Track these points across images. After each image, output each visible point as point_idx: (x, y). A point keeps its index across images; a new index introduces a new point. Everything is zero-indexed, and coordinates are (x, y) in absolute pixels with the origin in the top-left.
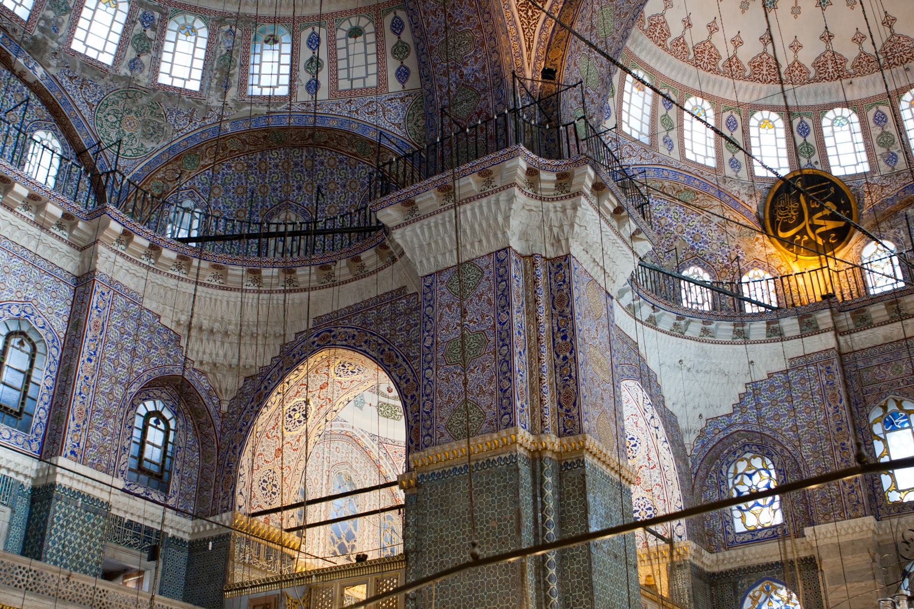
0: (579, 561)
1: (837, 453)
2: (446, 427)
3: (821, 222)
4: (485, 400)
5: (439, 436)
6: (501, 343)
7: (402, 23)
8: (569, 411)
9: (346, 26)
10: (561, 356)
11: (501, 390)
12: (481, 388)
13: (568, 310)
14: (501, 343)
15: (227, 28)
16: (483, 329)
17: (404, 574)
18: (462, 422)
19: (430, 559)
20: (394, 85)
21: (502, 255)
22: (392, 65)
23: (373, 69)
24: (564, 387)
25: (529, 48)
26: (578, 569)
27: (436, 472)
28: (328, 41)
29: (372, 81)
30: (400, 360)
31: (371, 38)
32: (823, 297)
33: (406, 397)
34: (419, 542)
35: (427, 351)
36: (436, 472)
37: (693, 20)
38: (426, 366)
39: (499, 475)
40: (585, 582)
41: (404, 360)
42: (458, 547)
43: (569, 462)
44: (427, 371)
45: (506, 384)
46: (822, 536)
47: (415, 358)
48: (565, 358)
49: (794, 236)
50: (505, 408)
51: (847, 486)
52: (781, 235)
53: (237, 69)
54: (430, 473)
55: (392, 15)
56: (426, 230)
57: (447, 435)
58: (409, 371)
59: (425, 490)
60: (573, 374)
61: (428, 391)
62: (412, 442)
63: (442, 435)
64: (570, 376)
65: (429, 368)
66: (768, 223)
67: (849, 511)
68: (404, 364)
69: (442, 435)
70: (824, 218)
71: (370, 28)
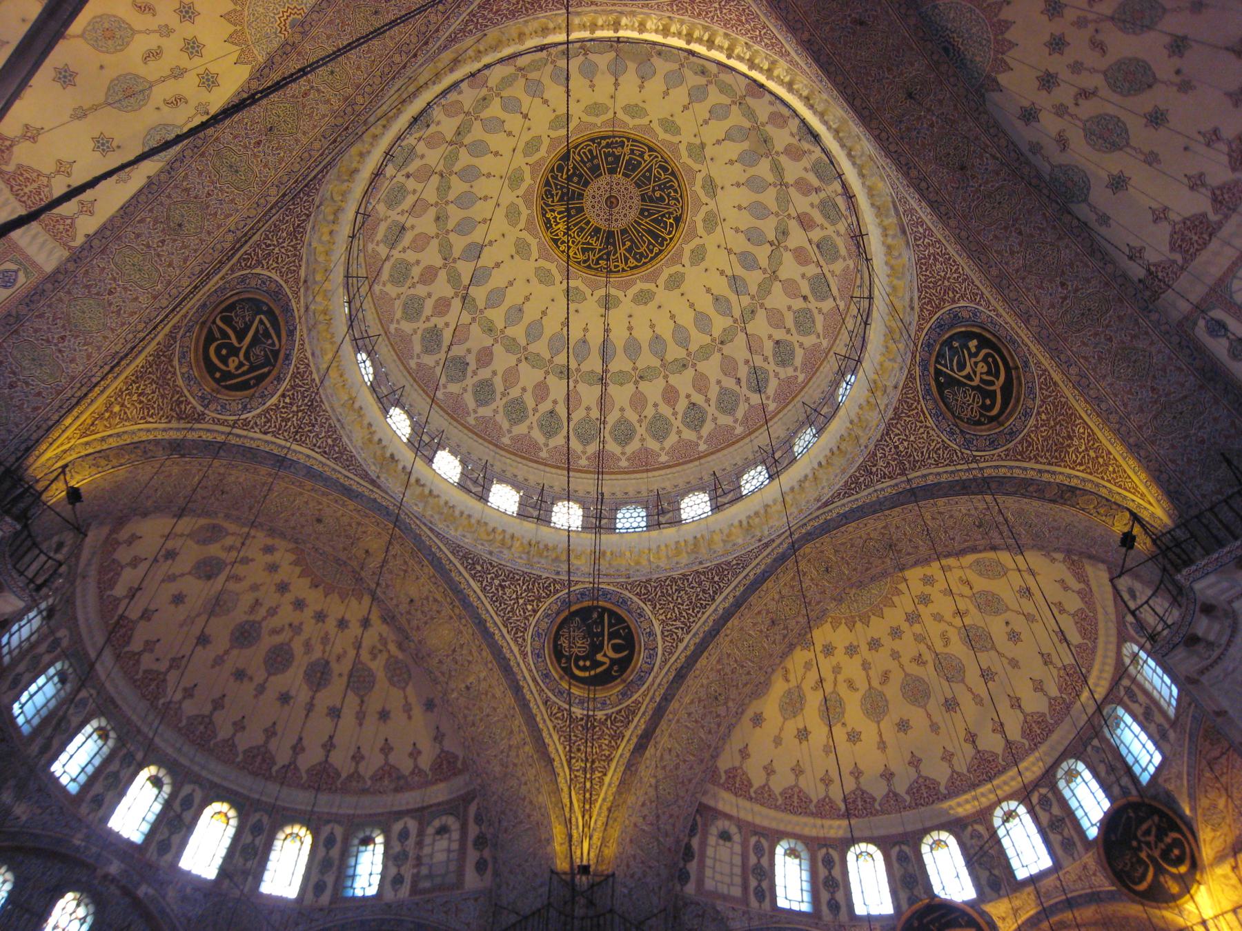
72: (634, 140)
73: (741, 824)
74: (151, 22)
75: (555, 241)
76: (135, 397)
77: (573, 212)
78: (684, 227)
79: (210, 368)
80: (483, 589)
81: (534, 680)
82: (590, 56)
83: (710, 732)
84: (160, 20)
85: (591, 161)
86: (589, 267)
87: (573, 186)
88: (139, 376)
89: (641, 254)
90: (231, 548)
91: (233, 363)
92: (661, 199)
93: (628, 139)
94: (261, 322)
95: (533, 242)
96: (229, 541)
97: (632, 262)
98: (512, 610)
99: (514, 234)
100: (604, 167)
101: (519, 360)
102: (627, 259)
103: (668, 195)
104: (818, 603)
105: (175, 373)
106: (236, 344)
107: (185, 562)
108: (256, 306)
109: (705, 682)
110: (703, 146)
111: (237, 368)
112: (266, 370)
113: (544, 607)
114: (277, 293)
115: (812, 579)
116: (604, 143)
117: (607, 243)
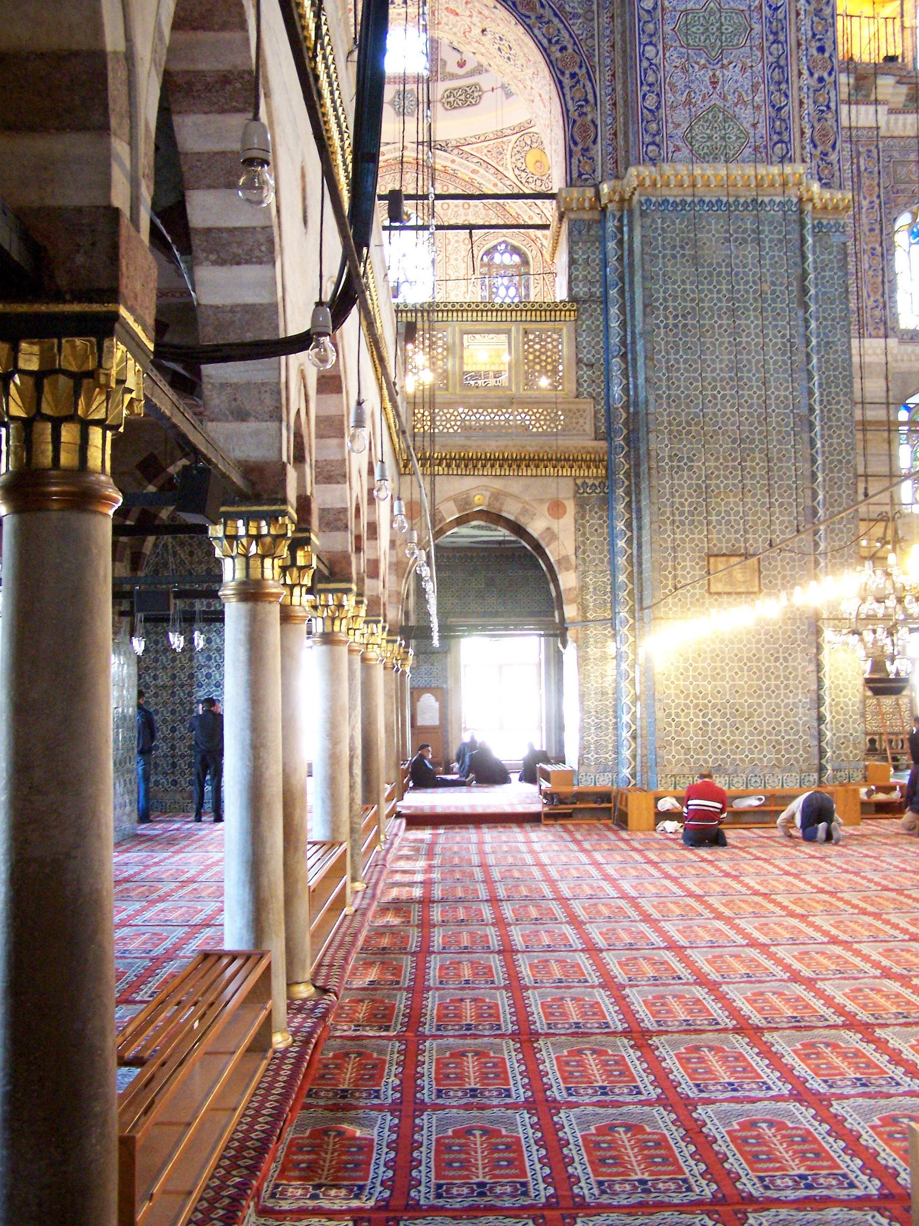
0: (836, 351)
1: (866, 258)
2: (684, 138)
4: (746, 115)
5: (671, 149)
6: (771, 37)
8: (826, 154)
10: (816, 76)
11: (773, 106)
12: (740, 96)
13: (827, 11)
14: (771, 37)
16: (742, 8)
17: (572, 329)
18: (710, 138)
19: (667, 318)
24: (819, 120)
26: (835, 360)
27: (671, 200)
30: (548, 13)
32: (890, 59)
33: (563, 73)
34: (647, 293)
35: (646, 17)
36: (671, 200)
38: (645, 40)
39: (770, 224)
40: (844, 377)
41: (556, 15)
42: (711, 309)
43: (825, 222)
44: (648, 48)
45: (780, 100)
46: (870, 352)
47: (576, 16)
48: (821, 80)
50: (779, 134)
51: (872, 299)
54: (660, 200)
57: (685, 152)
58: (567, 36)
59: (654, 221)
60: (833, 105)
61: (651, 79)
62: (576, 143)
63: (678, 149)
64: (828, 107)
65: (651, 43)
67: (870, 328)
68: (556, 21)
69: (678, 149)
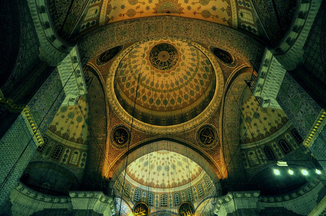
3: (143, 213)
7: (86, 155)
9: (75, 151)
15: (52, 142)
20: (80, 166)
21: (91, 211)
22: (81, 162)
23: (77, 161)
25: (107, 170)
28: (71, 152)
29: (76, 164)
31: (79, 155)
37: (133, 170)
49: (137, 215)
52: (135, 214)
53: (51, 151)
55: (84, 153)
56: (78, 200)
66: (134, 211)
70: (143, 213)
71: (79, 153)
72: (151, 63)
73: (238, 10)
74: (176, 160)
75: (177, 60)
76: (217, 157)
77: (170, 60)
78: (156, 45)
79: (212, 141)
80: (228, 77)
81: (236, 67)
82: (145, 84)
83: (219, 32)
84: (174, 159)
85: (161, 65)
86: (176, 51)
87: (167, 64)
88: (213, 156)
89: (167, 46)
90: (251, 114)
91: (210, 138)
92: (156, 51)
93: (152, 64)
94: (203, 134)
95: (180, 63)
96: (249, 115)
97: (169, 46)
98: (228, 71)
99: (181, 68)
100: (160, 62)
101: (199, 56)
102: (170, 47)
103: (154, 51)
104: (176, 22)
105: (214, 148)
106: (207, 138)
107: (257, 121)
108: (201, 136)
109: (209, 39)
110: (141, 56)
111: (211, 136)
112: (210, 130)
113: (224, 65)
114: (198, 132)
115: (172, 29)
116: (156, 66)
117: (170, 51)
